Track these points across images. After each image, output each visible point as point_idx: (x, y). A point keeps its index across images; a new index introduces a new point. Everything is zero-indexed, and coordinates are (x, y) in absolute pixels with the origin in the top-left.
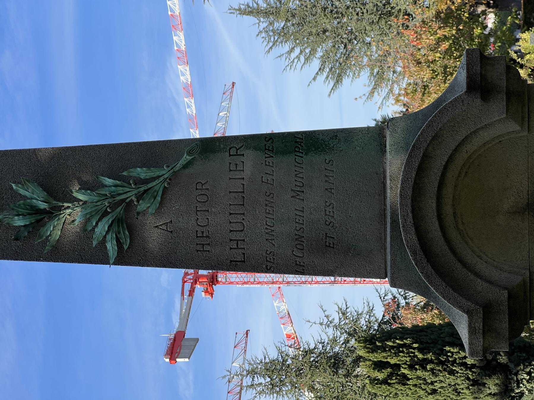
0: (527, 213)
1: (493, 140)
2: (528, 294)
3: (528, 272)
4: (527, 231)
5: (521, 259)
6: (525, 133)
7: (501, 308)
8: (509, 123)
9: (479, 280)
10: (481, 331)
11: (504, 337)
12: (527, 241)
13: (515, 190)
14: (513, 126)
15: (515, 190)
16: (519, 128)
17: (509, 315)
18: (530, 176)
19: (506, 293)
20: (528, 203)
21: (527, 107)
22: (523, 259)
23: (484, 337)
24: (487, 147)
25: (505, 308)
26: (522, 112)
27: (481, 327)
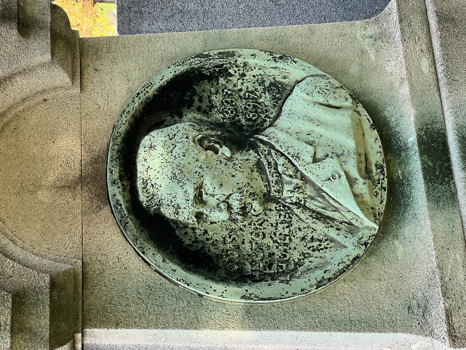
0: (79, 188)
1: (35, 95)
2: (80, 290)
3: (80, 262)
4: (79, 211)
5: (71, 246)
6: (77, 90)
7: (40, 297)
8: (56, 70)
9: (8, 260)
10: (8, 327)
11: (42, 339)
12: (80, 223)
13: (65, 160)
14: (60, 77)
15: (65, 160)
16: (68, 80)
17: (50, 306)
18: (83, 143)
19: (47, 279)
20: (81, 175)
21: (78, 60)
22: (73, 247)
23: (12, 337)
24: (27, 103)
25: (46, 298)
26: (73, 66)
27: (9, 322)
